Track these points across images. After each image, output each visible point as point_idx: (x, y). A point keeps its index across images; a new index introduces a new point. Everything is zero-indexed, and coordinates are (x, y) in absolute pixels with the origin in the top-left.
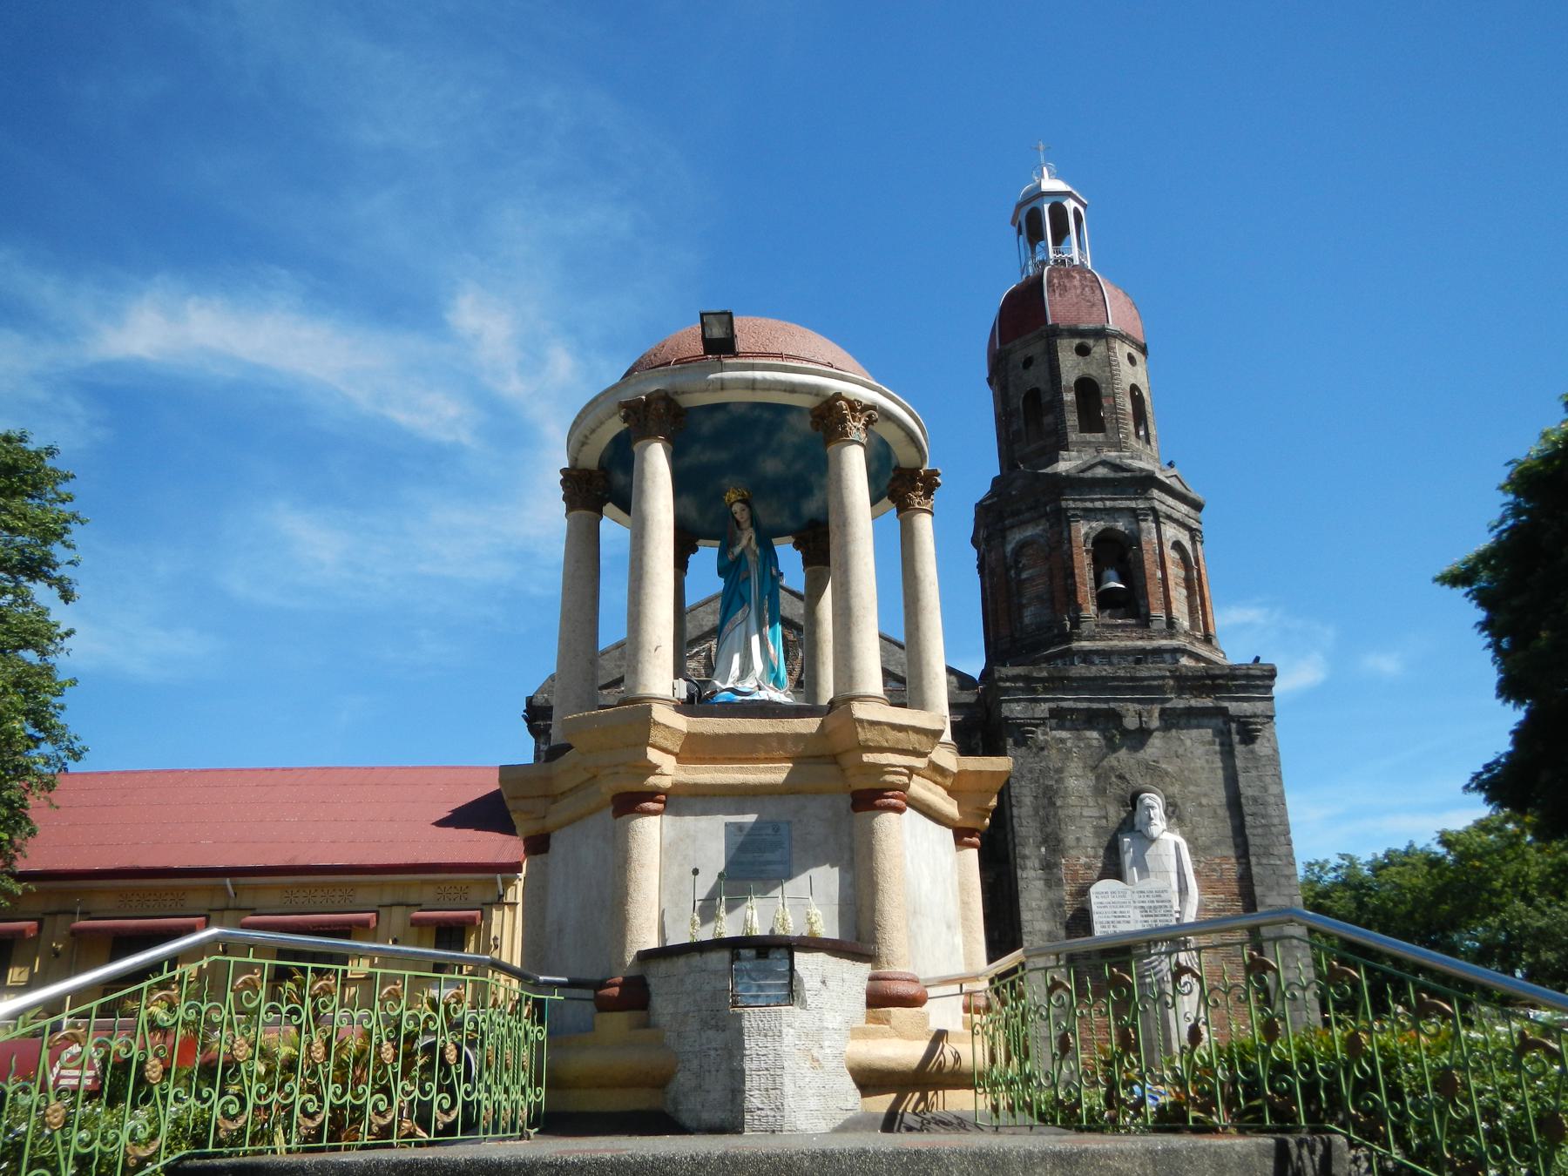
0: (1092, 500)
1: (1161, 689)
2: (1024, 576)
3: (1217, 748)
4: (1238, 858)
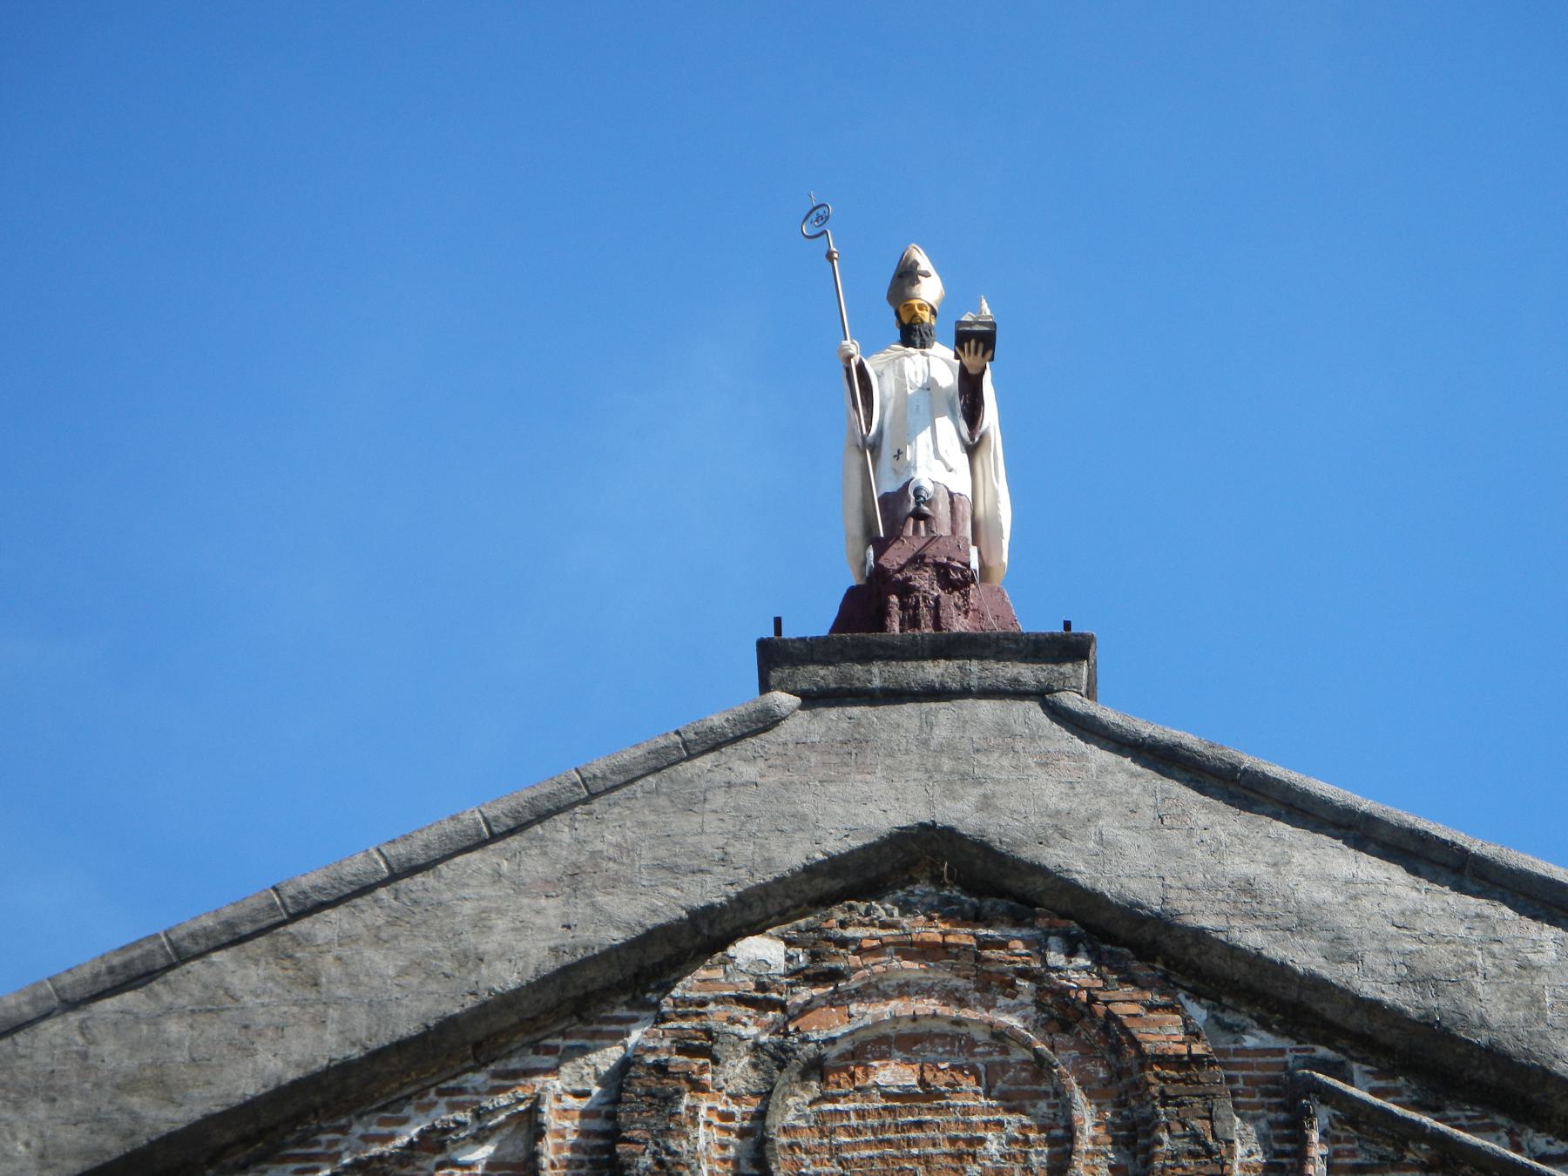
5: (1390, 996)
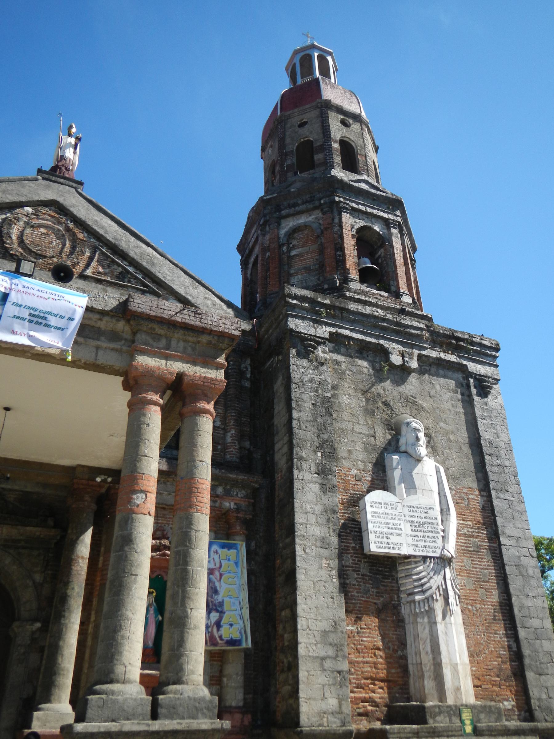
0: (358, 204)
1: (419, 337)
2: (293, 253)
3: (460, 397)
4: (480, 491)
5: (111, 240)
